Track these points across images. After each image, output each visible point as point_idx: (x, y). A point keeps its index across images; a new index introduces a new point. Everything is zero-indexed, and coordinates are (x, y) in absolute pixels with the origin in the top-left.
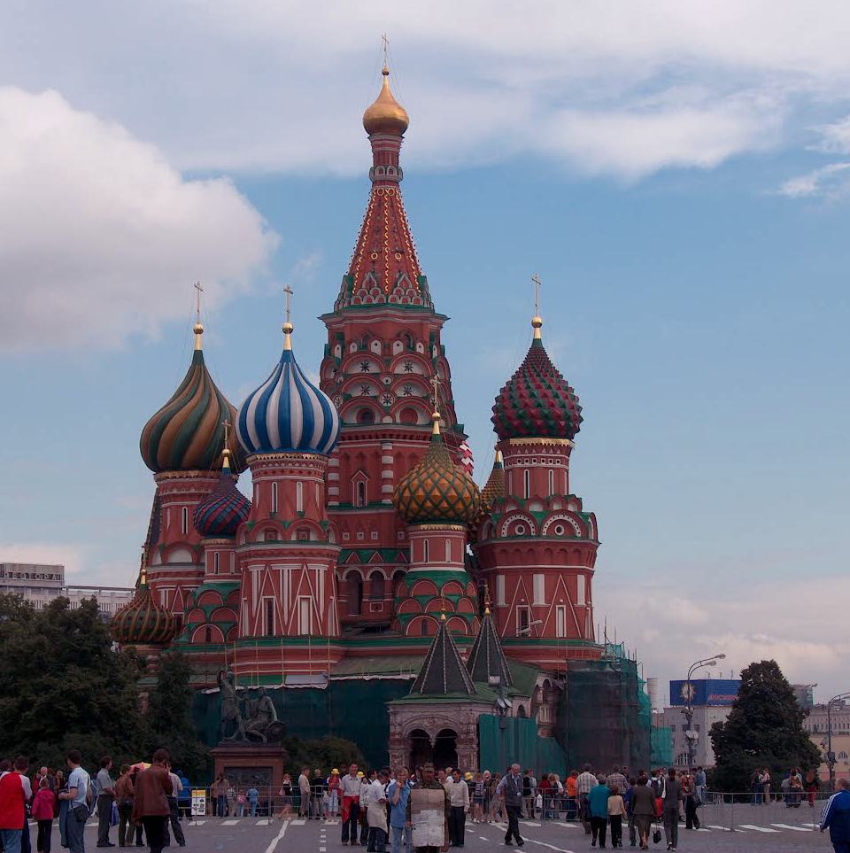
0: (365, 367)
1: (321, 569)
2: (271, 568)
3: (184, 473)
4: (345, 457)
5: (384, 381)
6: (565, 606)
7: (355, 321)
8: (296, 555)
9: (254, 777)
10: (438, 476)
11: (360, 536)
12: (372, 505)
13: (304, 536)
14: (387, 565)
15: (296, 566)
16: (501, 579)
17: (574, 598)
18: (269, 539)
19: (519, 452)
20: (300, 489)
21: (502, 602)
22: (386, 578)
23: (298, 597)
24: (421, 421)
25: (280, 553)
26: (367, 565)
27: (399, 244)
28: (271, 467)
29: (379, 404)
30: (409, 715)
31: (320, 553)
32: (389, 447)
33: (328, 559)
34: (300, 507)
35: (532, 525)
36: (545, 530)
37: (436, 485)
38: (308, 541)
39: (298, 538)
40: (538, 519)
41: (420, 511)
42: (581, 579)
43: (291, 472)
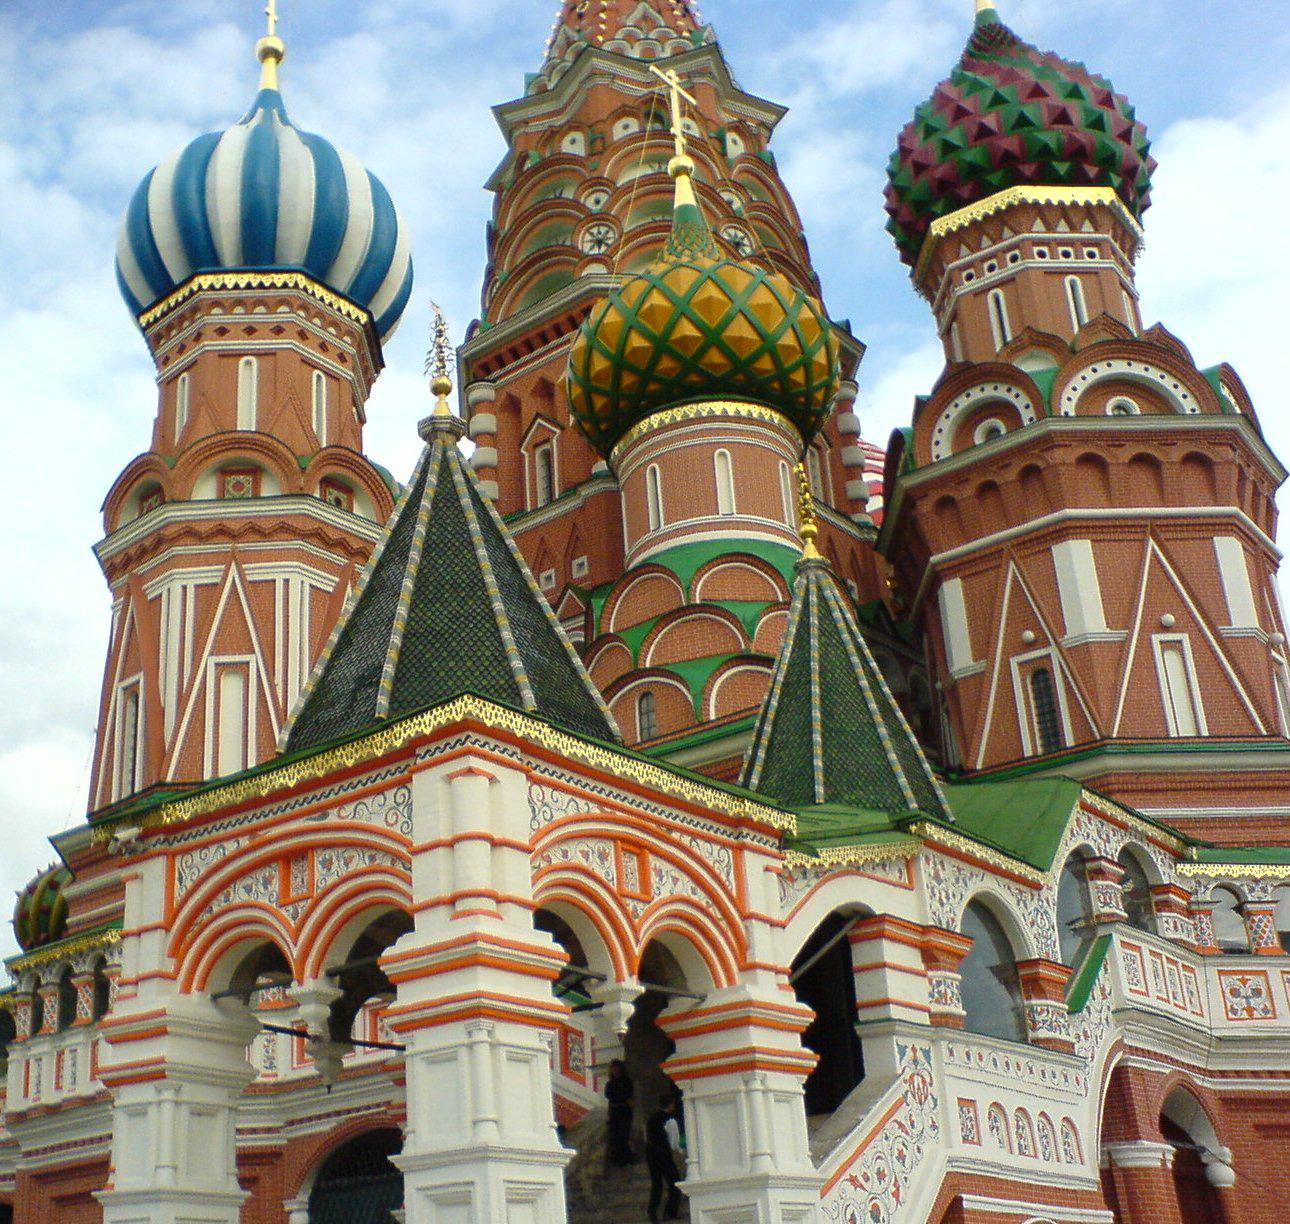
6: (1185, 638)
8: (201, 538)
13: (239, 486)
15: (208, 574)
16: (953, 593)
17: (1215, 609)
20: (248, 377)
21: (961, 657)
31: (284, 528)
33: (343, 561)
40: (1042, 386)
42: (1230, 552)
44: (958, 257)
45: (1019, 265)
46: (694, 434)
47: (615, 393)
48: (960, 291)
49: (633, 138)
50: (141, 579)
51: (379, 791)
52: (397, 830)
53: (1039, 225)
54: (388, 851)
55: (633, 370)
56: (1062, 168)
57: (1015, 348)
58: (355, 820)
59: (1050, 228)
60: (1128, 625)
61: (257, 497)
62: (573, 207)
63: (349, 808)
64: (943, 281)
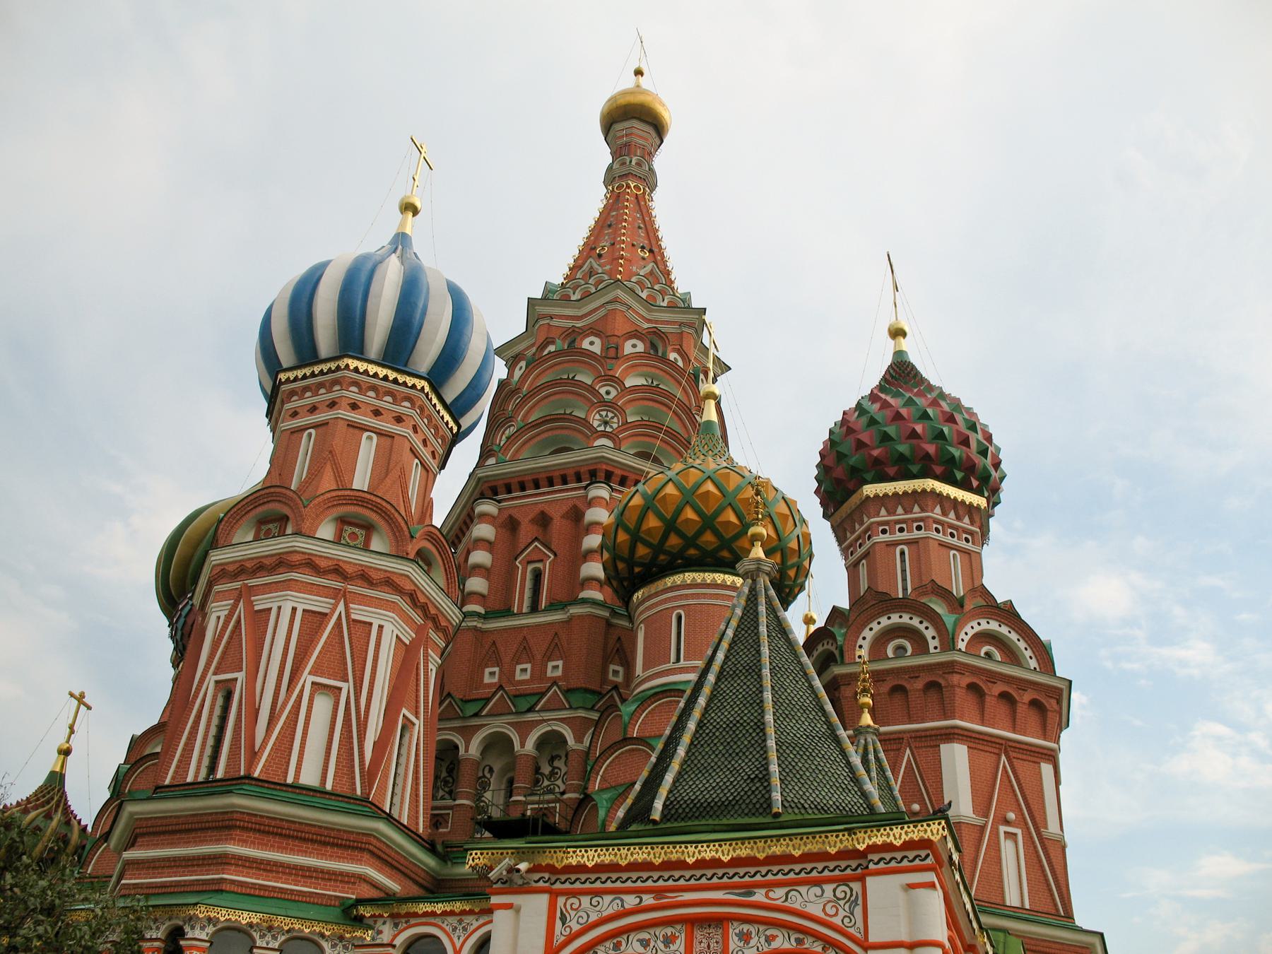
1: (390, 629)
2: (250, 604)
4: (510, 525)
5: (603, 391)
7: (555, 322)
11: (523, 672)
12: (553, 606)
14: (581, 713)
15: (319, 604)
19: (883, 512)
20: (368, 448)
22: (571, 741)
23: (307, 679)
25: (281, 562)
26: (531, 717)
28: (309, 399)
30: (608, 905)
31: (390, 583)
32: (601, 491)
33: (420, 621)
35: (929, 633)
41: (665, 537)
43: (354, 406)
44: (878, 515)
45: (922, 534)
46: (717, 596)
47: (658, 549)
48: (877, 539)
49: (638, 356)
50: (252, 590)
51: (817, 883)
52: (837, 921)
53: (938, 510)
54: (817, 936)
55: (681, 534)
56: (915, 469)
57: (921, 589)
58: (786, 904)
59: (945, 514)
60: (987, 816)
61: (366, 548)
62: (588, 391)
63: (779, 893)
64: (859, 529)
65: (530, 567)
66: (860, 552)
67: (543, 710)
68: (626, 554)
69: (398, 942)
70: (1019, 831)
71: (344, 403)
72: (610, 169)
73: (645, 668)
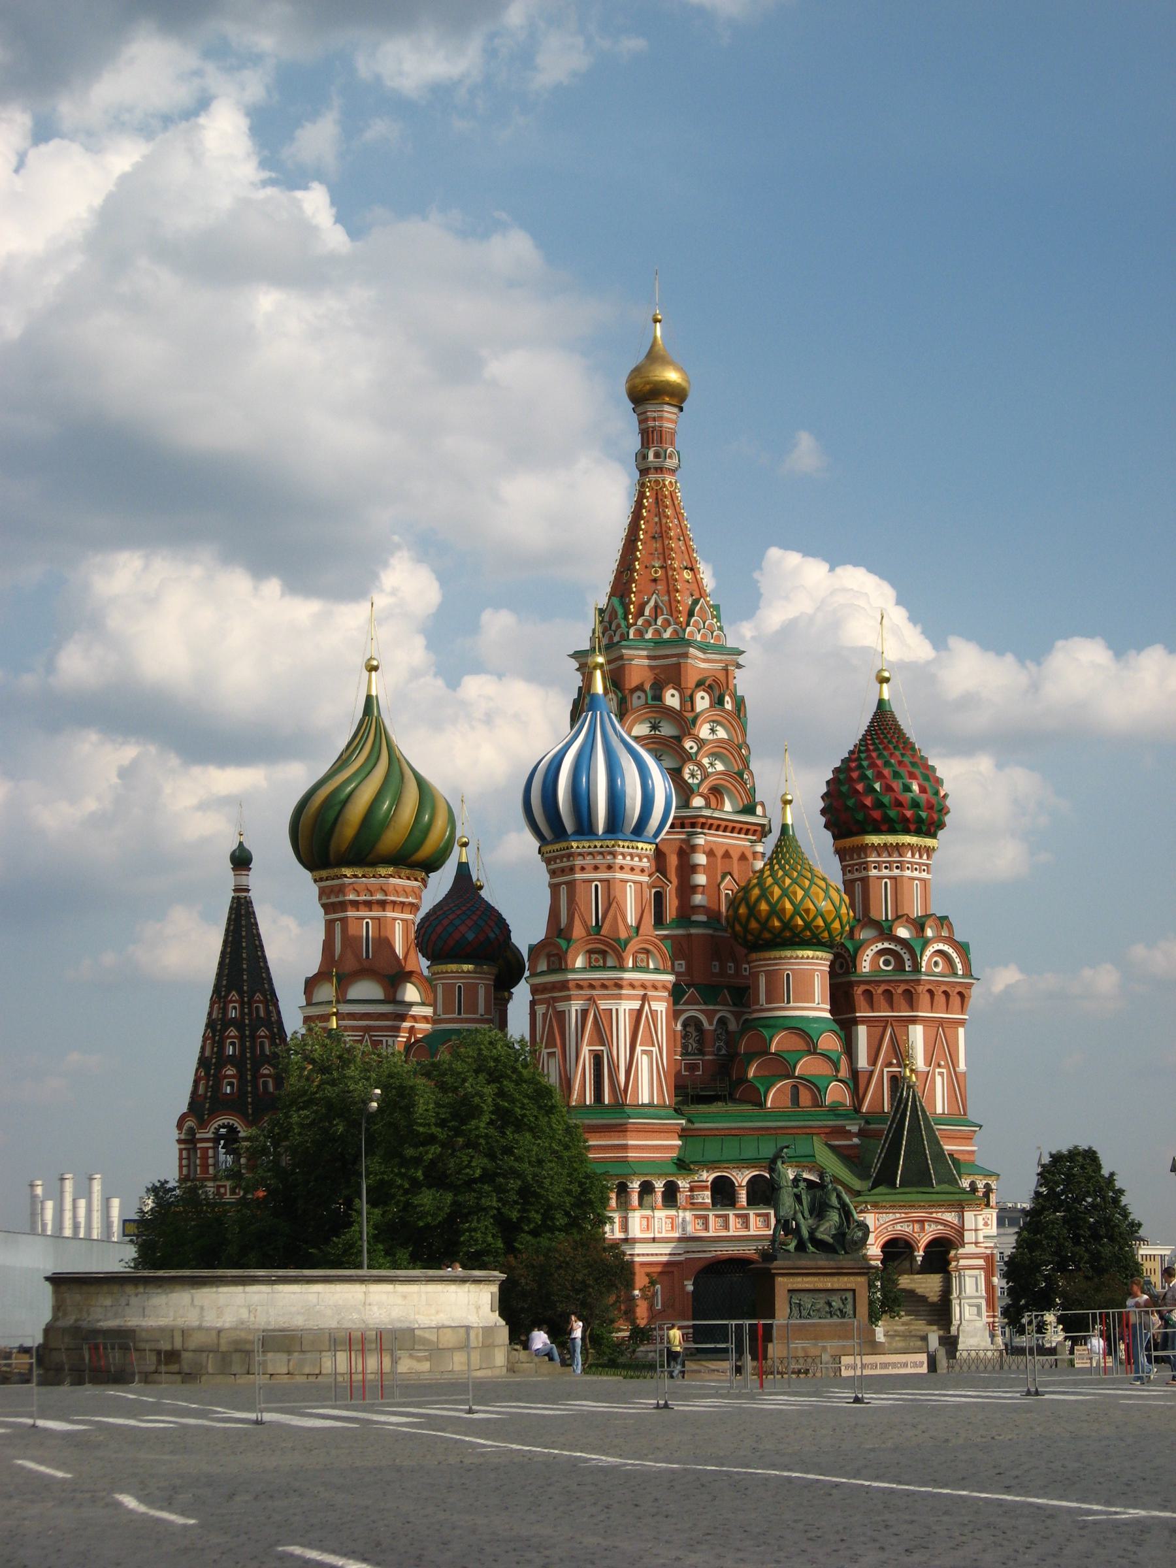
0: (654, 727)
3: (369, 870)
9: (830, 1305)
10: (788, 881)
13: (642, 960)
14: (711, 1007)
16: (862, 1031)
18: (594, 963)
21: (863, 1062)
23: (639, 1049)
24: (728, 807)
27: (687, 557)
29: (685, 782)
30: (891, 1216)
32: (700, 841)
34: (631, 919)
35: (906, 957)
36: (924, 964)
37: (785, 893)
38: (646, 970)
39: (635, 961)
53: (909, 854)
65: (654, 891)
66: (857, 875)
67: (684, 1004)
68: (744, 920)
69: (710, 1179)
70: (944, 1070)
71: (617, 867)
72: (642, 456)
73: (768, 1001)
